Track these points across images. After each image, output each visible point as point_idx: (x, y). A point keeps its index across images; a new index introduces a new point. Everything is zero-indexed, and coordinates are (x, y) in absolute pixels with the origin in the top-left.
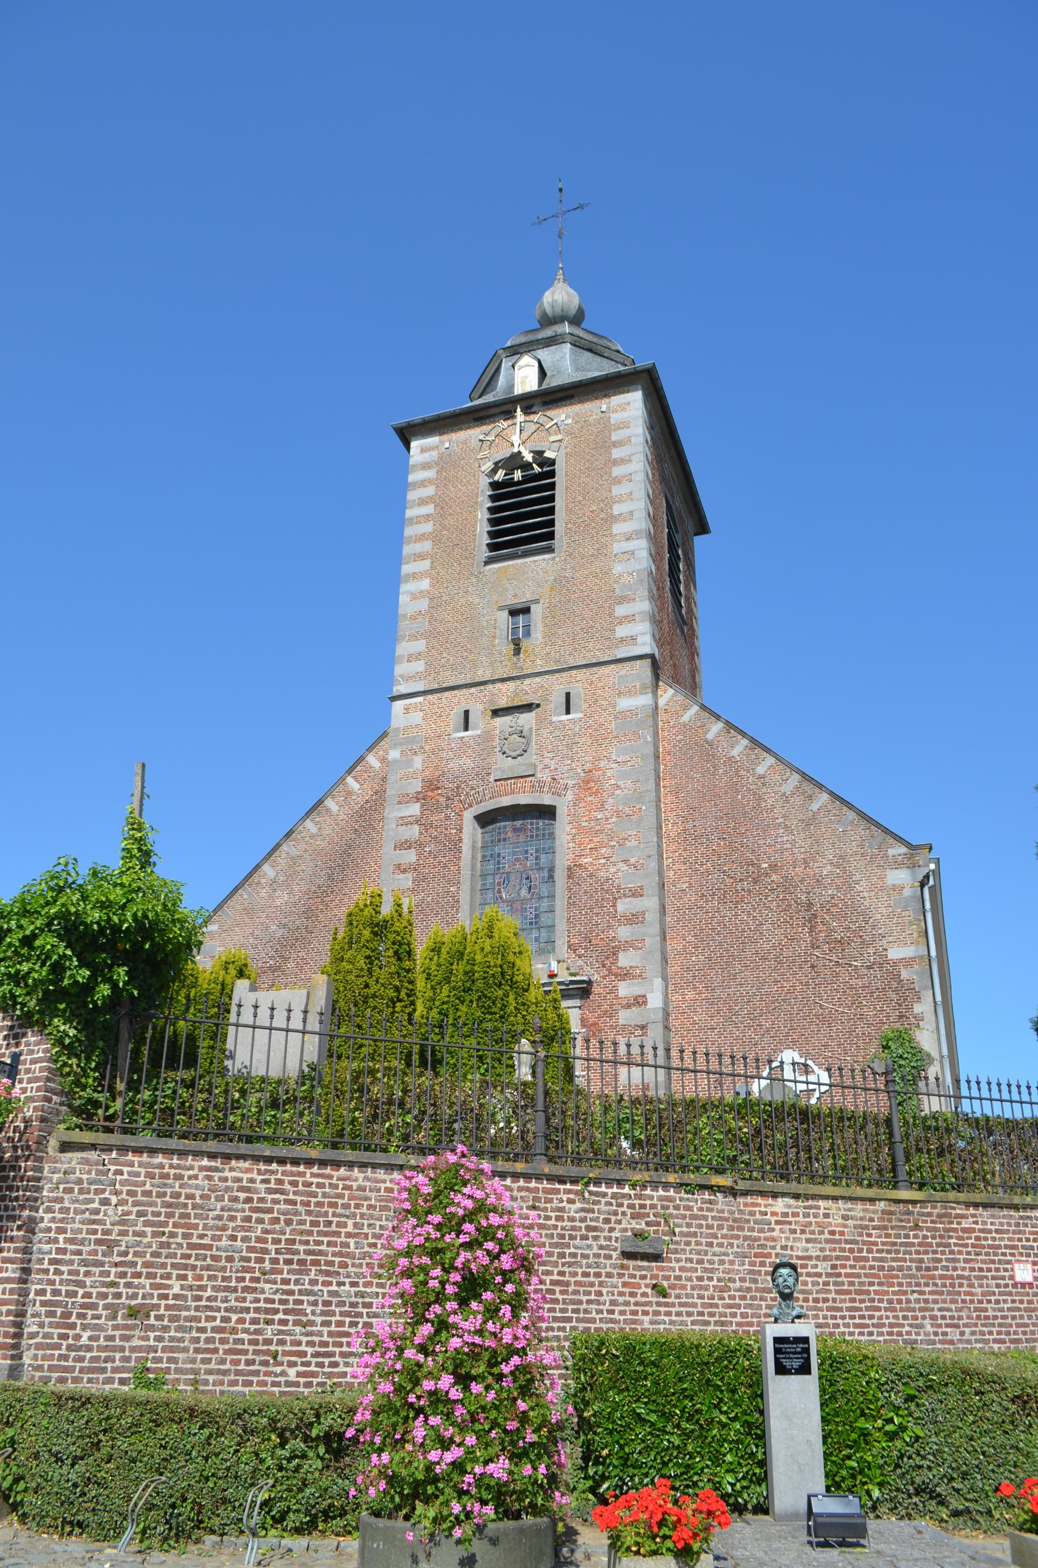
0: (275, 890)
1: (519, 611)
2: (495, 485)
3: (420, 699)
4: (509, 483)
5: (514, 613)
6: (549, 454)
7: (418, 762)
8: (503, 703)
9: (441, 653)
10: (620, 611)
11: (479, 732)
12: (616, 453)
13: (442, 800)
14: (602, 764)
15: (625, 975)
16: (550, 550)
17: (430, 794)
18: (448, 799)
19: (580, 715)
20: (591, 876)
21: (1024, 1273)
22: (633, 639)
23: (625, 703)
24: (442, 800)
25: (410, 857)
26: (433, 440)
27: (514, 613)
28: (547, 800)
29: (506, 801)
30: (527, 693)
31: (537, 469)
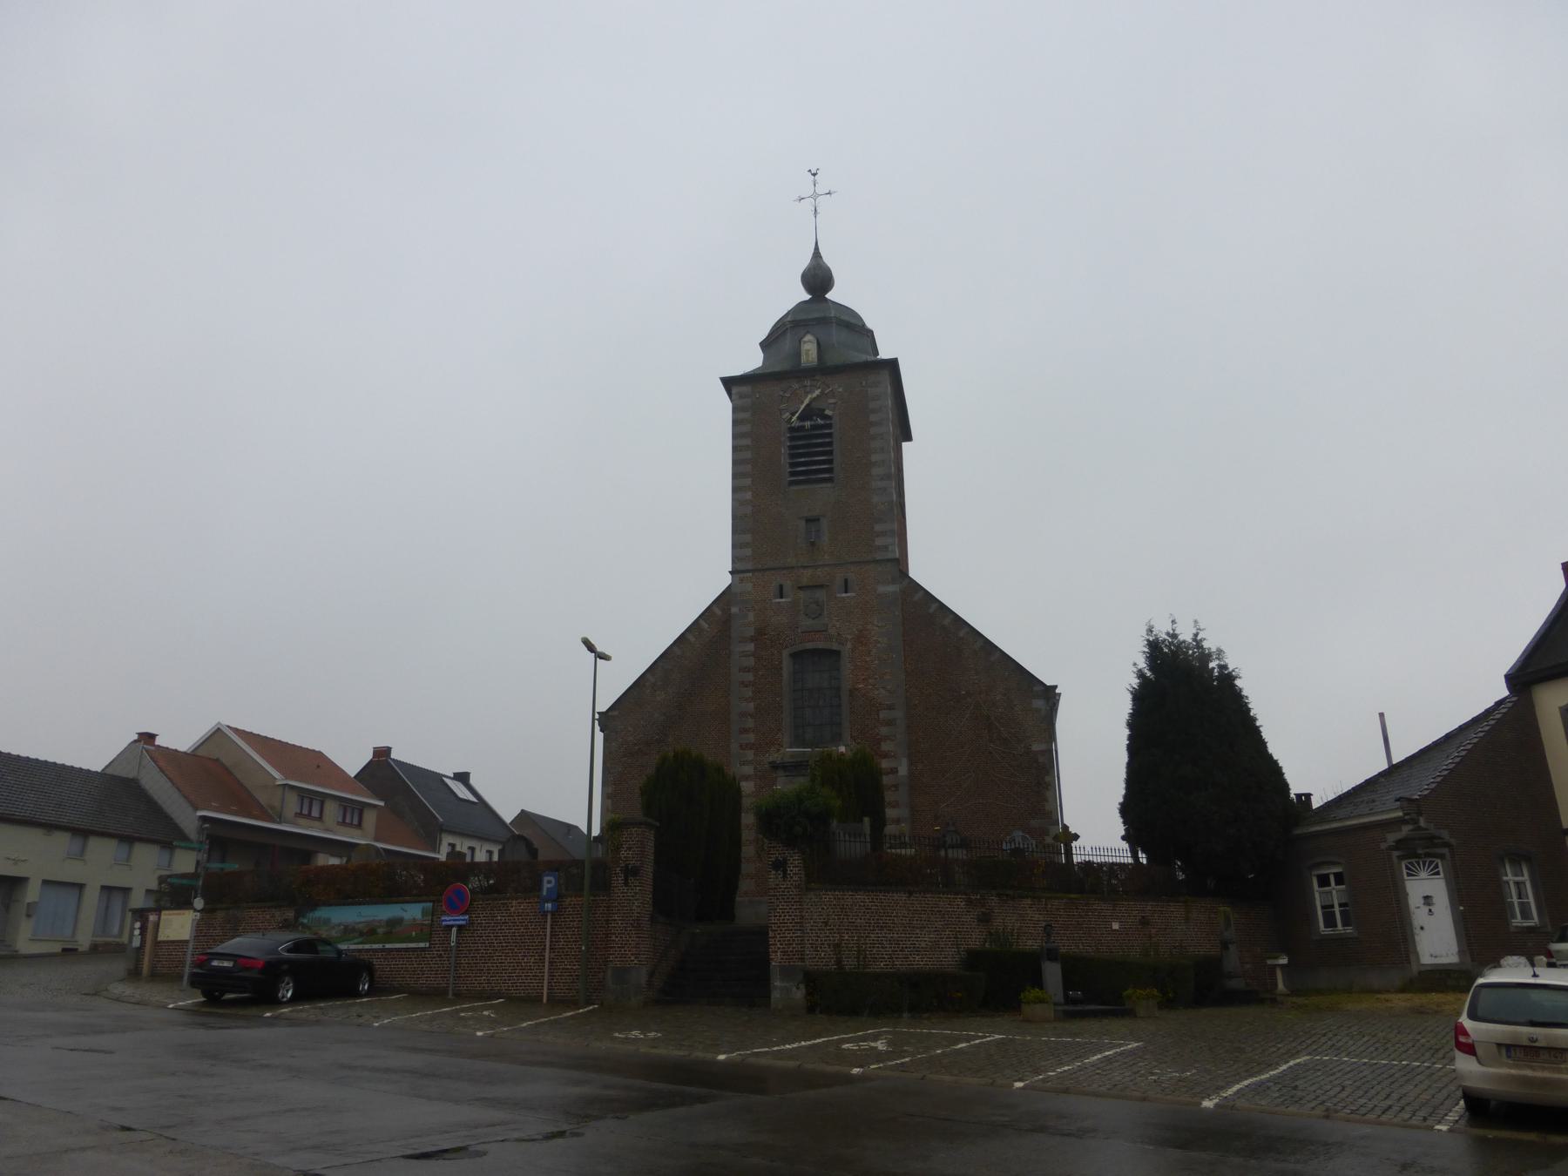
4: (801, 428)
5: (808, 521)
6: (828, 412)
7: (751, 617)
8: (805, 582)
10: (878, 528)
12: (873, 418)
15: (885, 756)
16: (830, 480)
21: (1116, 926)
22: (886, 548)
23: (882, 589)
25: (750, 677)
27: (808, 521)
28: (835, 647)
29: (810, 646)
31: (820, 421)
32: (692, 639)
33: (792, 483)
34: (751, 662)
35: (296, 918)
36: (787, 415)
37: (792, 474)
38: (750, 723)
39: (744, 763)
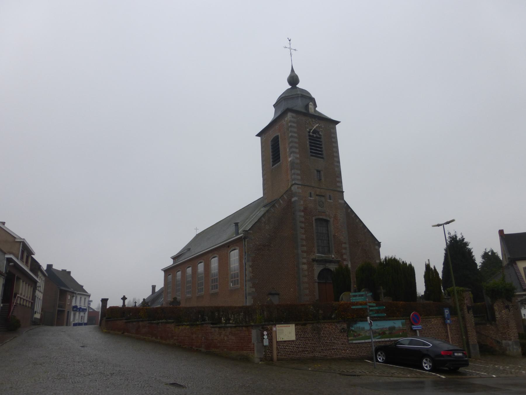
1: (319, 171)
2: (310, 136)
7: (302, 202)
8: (318, 193)
15: (345, 260)
16: (323, 158)
25: (303, 225)
26: (294, 115)
28: (328, 219)
29: (321, 217)
31: (318, 136)
32: (277, 206)
33: (312, 156)
34: (303, 219)
35: (348, 327)
36: (308, 130)
37: (311, 152)
38: (304, 243)
39: (303, 258)
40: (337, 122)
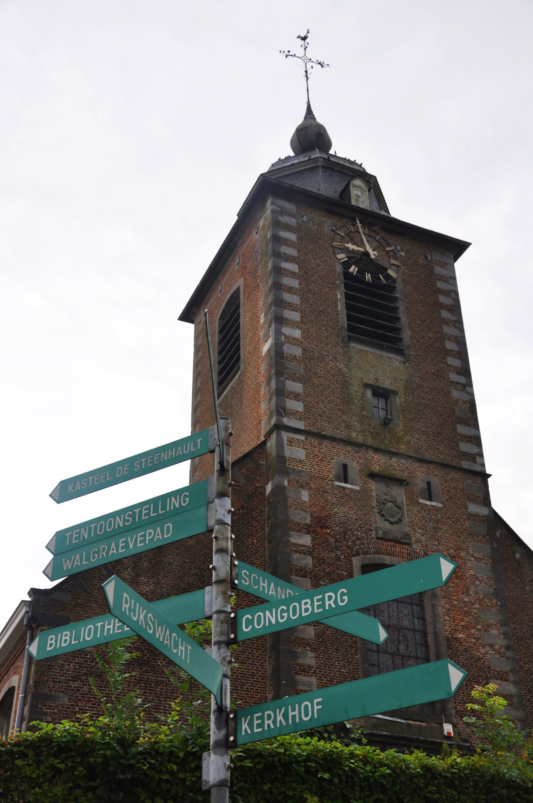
0: (138, 575)
2: (347, 275)
3: (302, 438)
6: (390, 272)
8: (376, 468)
9: (317, 402)
11: (358, 488)
13: (332, 540)
14: (463, 554)
17: (319, 530)
18: (337, 541)
19: (440, 505)
20: (466, 650)
24: (332, 540)
30: (395, 469)
40: (458, 247)
